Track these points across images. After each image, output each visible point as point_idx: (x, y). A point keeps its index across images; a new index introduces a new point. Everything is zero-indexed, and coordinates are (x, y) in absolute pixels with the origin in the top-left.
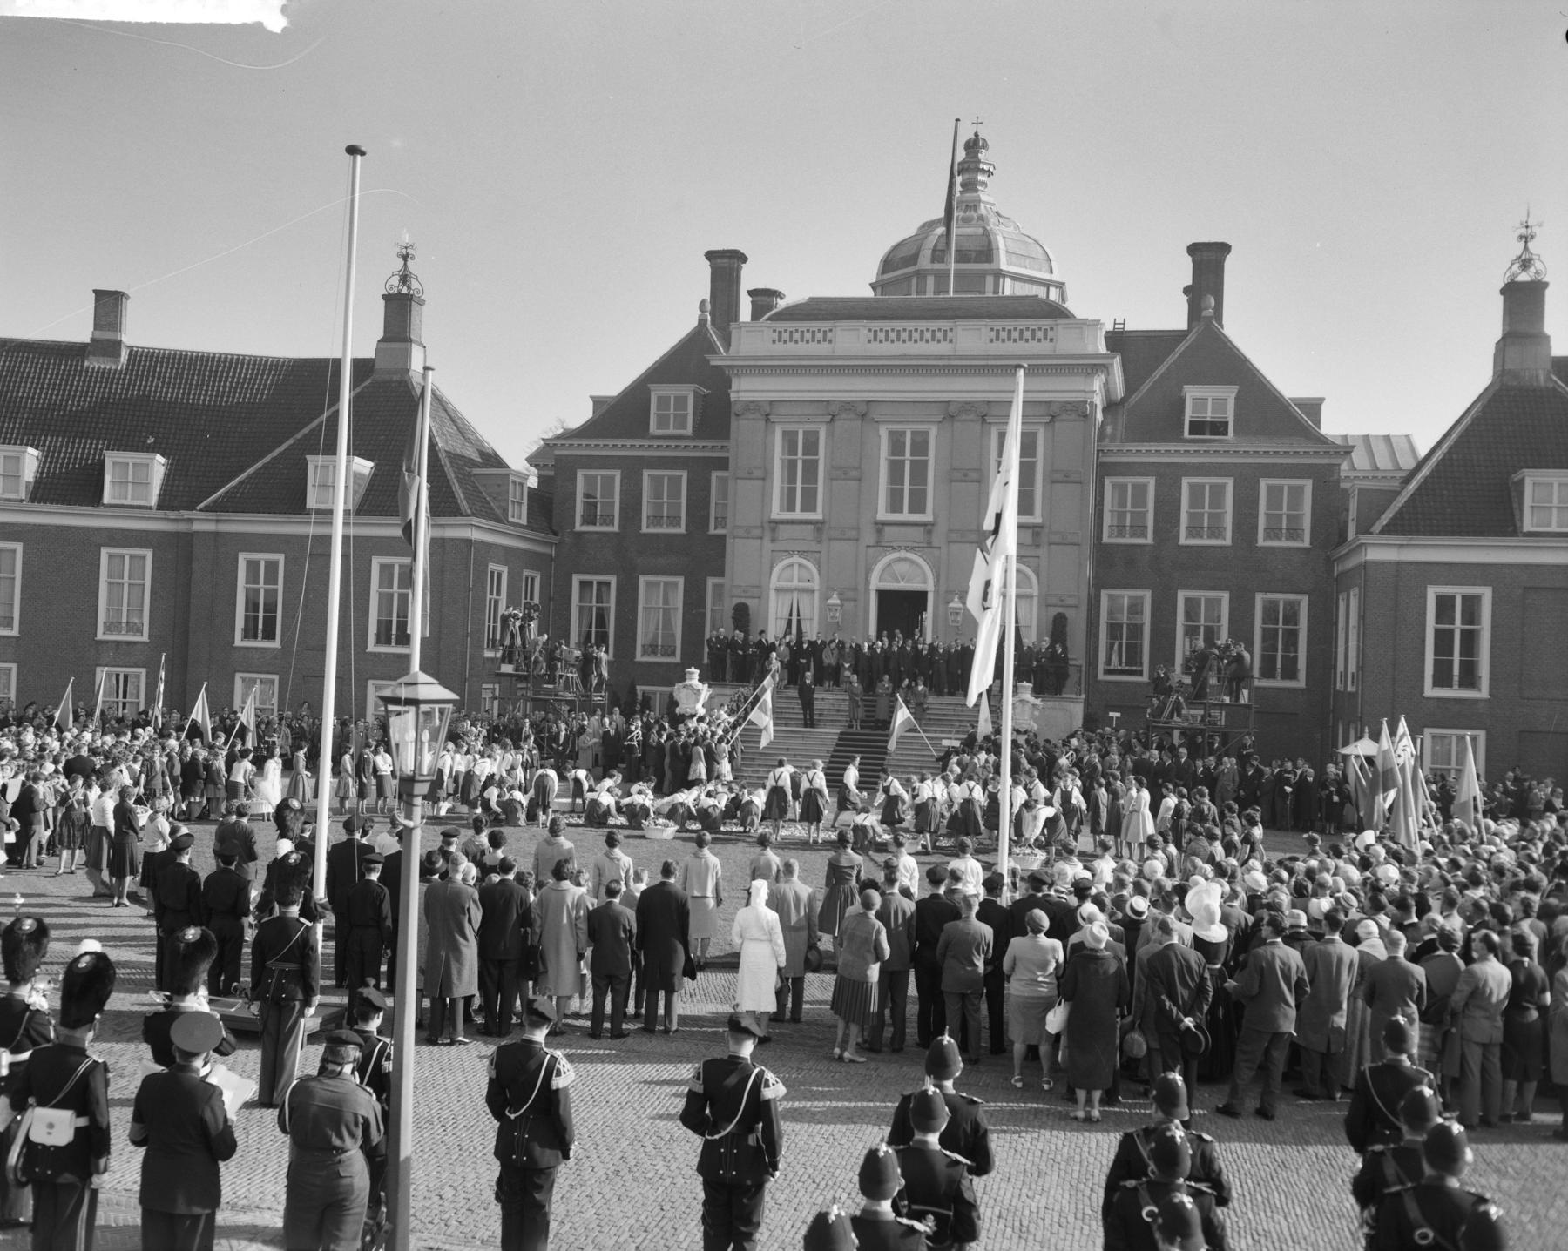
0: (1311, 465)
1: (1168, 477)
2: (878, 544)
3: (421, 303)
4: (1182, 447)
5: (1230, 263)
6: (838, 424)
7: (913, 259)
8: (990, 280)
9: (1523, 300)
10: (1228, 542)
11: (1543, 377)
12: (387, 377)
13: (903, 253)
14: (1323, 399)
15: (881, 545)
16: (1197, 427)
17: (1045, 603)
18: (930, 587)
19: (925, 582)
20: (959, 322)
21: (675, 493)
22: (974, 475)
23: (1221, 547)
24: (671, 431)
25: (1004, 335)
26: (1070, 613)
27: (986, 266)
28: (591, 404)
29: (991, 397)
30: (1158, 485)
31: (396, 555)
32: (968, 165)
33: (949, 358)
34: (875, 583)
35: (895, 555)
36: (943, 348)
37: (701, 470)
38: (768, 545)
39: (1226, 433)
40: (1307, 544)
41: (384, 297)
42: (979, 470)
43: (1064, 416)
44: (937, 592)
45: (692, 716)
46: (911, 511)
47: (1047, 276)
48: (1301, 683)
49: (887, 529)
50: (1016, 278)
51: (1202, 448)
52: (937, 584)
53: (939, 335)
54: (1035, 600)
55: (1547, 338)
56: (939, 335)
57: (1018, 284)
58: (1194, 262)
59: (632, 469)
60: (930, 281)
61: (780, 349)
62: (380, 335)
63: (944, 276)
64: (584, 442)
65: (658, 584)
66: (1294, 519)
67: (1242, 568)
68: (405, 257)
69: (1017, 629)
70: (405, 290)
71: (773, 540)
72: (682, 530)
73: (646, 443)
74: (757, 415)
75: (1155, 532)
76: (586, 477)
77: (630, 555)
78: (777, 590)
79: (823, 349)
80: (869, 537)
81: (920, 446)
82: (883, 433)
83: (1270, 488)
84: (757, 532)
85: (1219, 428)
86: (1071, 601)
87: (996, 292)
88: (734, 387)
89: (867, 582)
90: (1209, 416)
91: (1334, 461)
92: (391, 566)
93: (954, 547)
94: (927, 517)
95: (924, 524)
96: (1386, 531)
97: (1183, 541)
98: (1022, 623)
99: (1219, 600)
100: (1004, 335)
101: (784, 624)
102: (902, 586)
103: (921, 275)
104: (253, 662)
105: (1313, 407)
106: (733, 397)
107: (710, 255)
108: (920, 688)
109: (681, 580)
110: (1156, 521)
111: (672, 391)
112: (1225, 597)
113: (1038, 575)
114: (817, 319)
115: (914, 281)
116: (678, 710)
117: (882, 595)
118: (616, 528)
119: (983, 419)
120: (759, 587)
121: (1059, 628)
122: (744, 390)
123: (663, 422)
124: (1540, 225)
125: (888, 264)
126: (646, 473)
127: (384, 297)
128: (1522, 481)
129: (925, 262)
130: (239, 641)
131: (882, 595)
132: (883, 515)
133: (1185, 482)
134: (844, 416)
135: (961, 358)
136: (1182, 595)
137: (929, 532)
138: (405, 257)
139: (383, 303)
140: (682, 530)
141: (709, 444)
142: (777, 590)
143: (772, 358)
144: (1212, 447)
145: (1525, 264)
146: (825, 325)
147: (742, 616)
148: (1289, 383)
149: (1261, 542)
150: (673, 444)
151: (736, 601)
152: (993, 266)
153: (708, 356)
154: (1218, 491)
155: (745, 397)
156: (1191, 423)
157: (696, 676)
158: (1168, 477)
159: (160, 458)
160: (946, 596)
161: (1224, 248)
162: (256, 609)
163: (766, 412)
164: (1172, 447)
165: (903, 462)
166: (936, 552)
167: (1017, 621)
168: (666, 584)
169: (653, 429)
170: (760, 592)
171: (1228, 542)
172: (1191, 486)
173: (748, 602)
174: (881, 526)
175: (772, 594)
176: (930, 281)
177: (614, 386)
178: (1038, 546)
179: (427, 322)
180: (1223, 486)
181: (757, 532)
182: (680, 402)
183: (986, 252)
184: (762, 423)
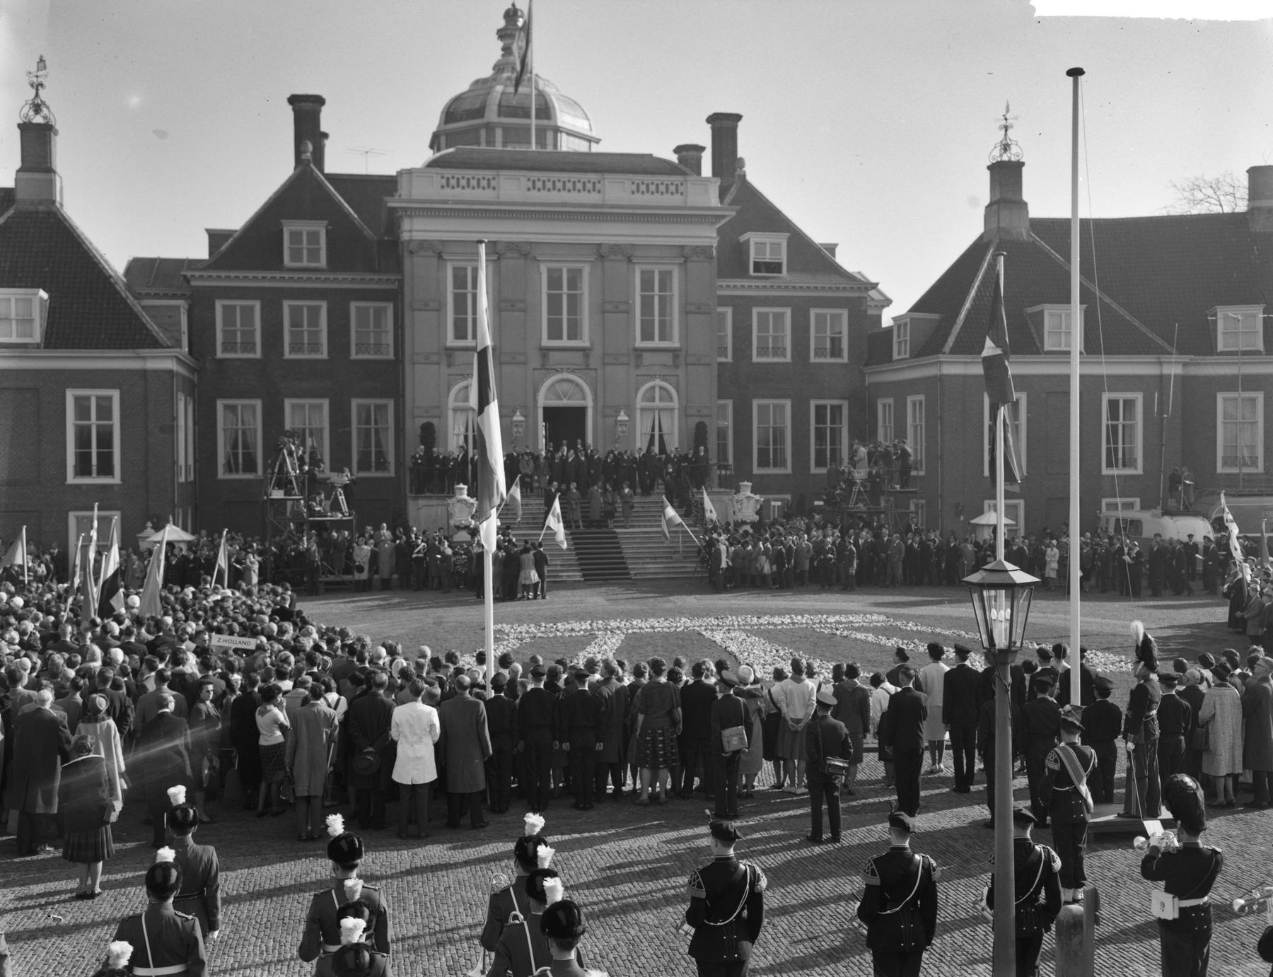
0: (792, 297)
1: (742, 306)
2: (543, 367)
3: (56, 133)
4: (746, 283)
5: (742, 128)
6: (504, 262)
7: (480, 112)
8: (550, 135)
9: (1006, 176)
10: (788, 359)
11: (1024, 233)
12: (32, 208)
13: (467, 106)
14: (836, 245)
15: (546, 368)
16: (758, 267)
17: (685, 413)
18: (589, 403)
19: (584, 398)
20: (607, 176)
21: (314, 321)
22: (623, 307)
23: (783, 364)
24: (305, 263)
25: (643, 188)
26: (706, 420)
27: (545, 122)
28: (206, 237)
29: (534, 238)
30: (734, 314)
31: (93, 387)
32: (514, 29)
33: (596, 206)
34: (542, 402)
35: (558, 376)
36: (593, 198)
37: (338, 301)
38: (444, 370)
39: (780, 272)
40: (845, 359)
41: (19, 126)
42: (627, 303)
43: (694, 258)
44: (595, 408)
45: (467, 528)
46: (570, 338)
47: (588, 133)
48: (789, 470)
49: (552, 354)
50: (571, 134)
51: (761, 283)
52: (595, 400)
53: (589, 186)
54: (676, 413)
55: (1026, 204)
56: (589, 186)
57: (571, 139)
58: (713, 129)
59: (271, 300)
60: (499, 133)
61: (448, 193)
62: (18, 164)
63: (494, 126)
64: (214, 274)
65: (303, 407)
66: (836, 342)
67: (797, 380)
68: (38, 86)
69: (661, 436)
70: (38, 120)
71: (449, 365)
72: (324, 355)
73: (278, 275)
74: (430, 253)
75: (735, 350)
76: (224, 307)
77: (271, 379)
78: (455, 410)
79: (488, 195)
80: (535, 361)
81: (574, 282)
82: (543, 269)
83: (817, 316)
84: (435, 358)
85: (775, 267)
86: (705, 412)
87: (555, 146)
88: (406, 224)
89: (535, 401)
90: (768, 257)
91: (863, 295)
92: (88, 398)
93: (609, 368)
94: (584, 342)
95: (583, 350)
96: (954, 351)
97: (755, 359)
98: (665, 430)
99: (783, 406)
100: (643, 188)
101: (462, 439)
102: (565, 403)
103: (490, 127)
104: (83, 498)
105: (832, 248)
106: (405, 236)
107: (293, 100)
108: (627, 490)
109: (326, 403)
110: (734, 343)
111: (305, 227)
112: (788, 404)
113: (678, 391)
114: (586, 171)
115: (483, 132)
116: (452, 522)
117: (546, 410)
118: (258, 354)
119: (629, 260)
120: (438, 407)
121: (700, 434)
122: (415, 230)
123: (296, 255)
124: (1016, 118)
125: (450, 114)
126: (286, 304)
127: (19, 126)
128: (1042, 312)
129: (492, 115)
130: (71, 479)
131: (546, 410)
132: (546, 342)
133: (755, 311)
134: (509, 255)
135: (612, 207)
136: (756, 403)
137: (587, 356)
138: (38, 86)
139: (18, 132)
140: (324, 355)
141: (349, 276)
142: (455, 410)
143: (524, 204)
144: (768, 283)
145: (1006, 147)
146: (489, 173)
147: (429, 434)
148: (818, 235)
149: (813, 359)
150: (305, 276)
151: (420, 422)
152: (551, 123)
153: (386, 199)
154: (779, 317)
155: (418, 236)
156: (756, 264)
157: (465, 492)
158: (742, 306)
159: (43, 294)
160: (607, 411)
161: (738, 117)
162: (88, 444)
163: (438, 251)
164: (739, 282)
165: (561, 295)
166: (593, 373)
167: (660, 429)
168: (311, 406)
169: (287, 261)
170: (439, 410)
171: (788, 359)
172: (759, 314)
173: (435, 421)
174: (545, 352)
175: (450, 413)
176: (499, 133)
177: (236, 218)
178: (676, 366)
179: (63, 154)
180: (783, 314)
181: (435, 358)
182: (313, 237)
183: (545, 111)
184: (435, 260)
